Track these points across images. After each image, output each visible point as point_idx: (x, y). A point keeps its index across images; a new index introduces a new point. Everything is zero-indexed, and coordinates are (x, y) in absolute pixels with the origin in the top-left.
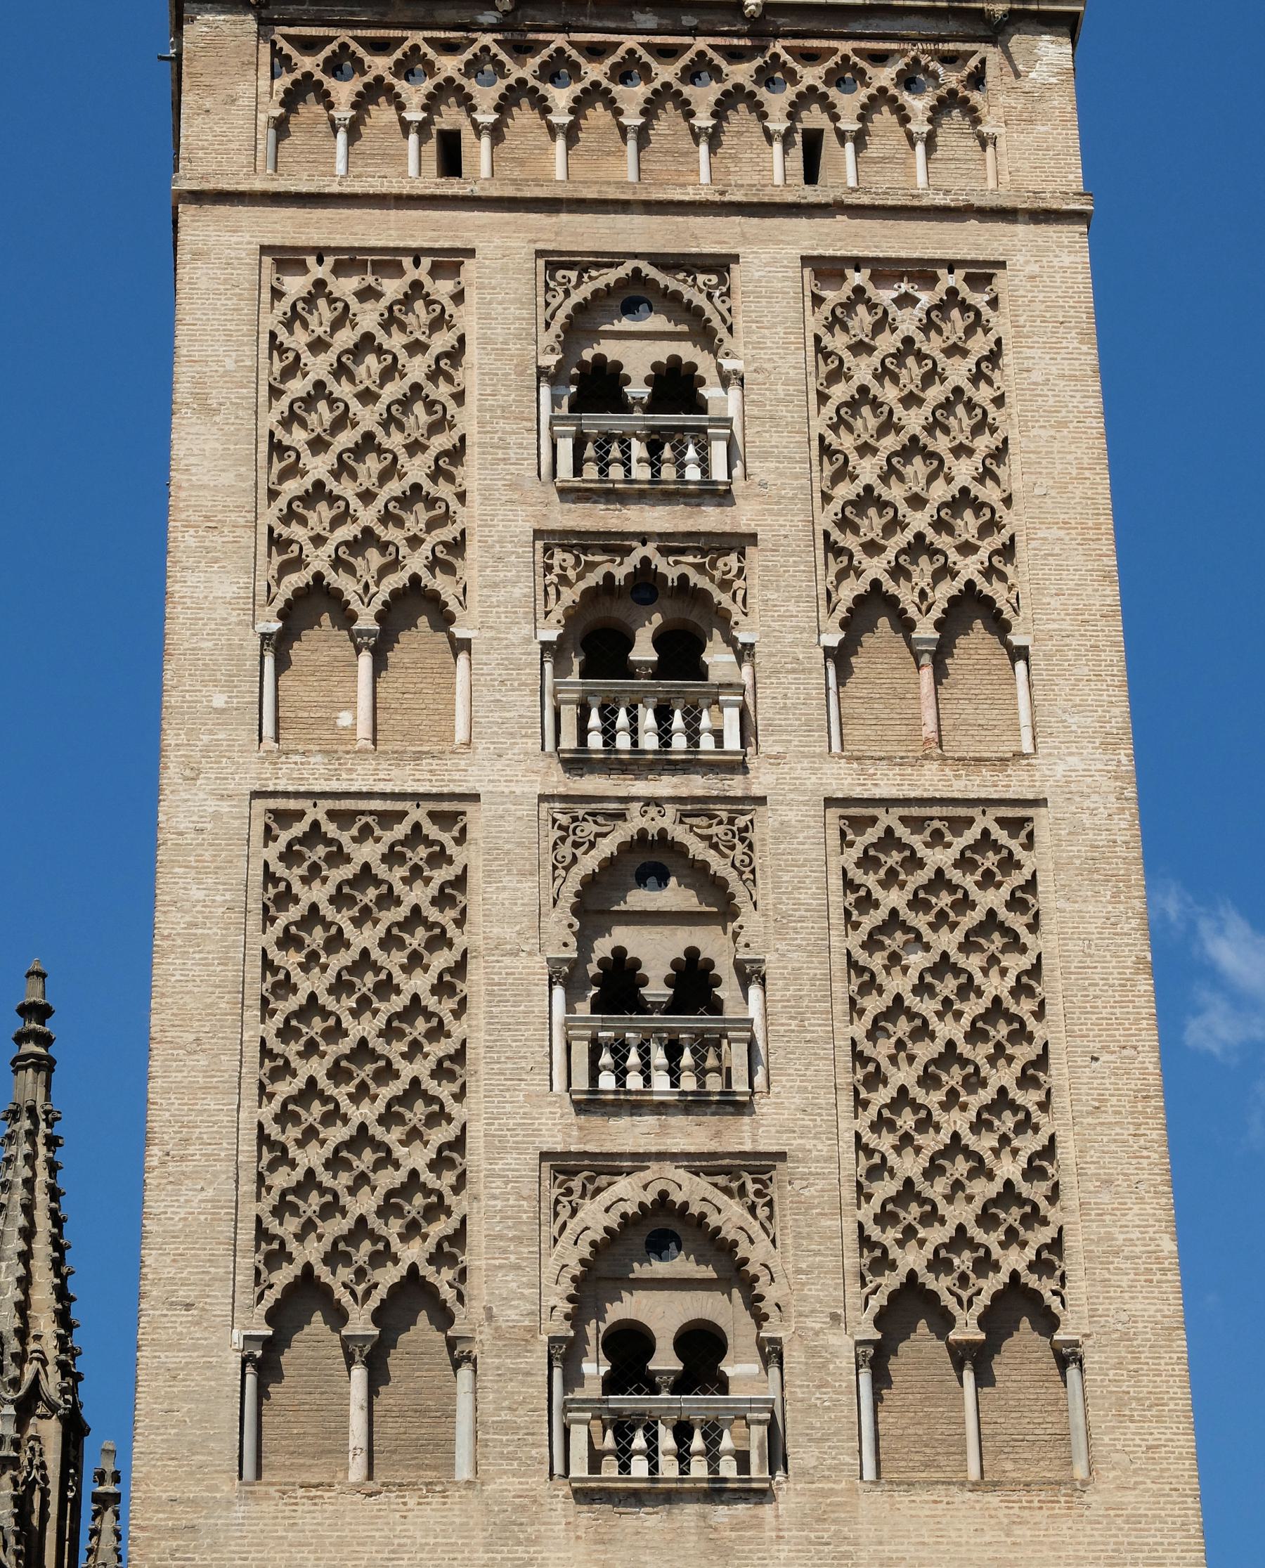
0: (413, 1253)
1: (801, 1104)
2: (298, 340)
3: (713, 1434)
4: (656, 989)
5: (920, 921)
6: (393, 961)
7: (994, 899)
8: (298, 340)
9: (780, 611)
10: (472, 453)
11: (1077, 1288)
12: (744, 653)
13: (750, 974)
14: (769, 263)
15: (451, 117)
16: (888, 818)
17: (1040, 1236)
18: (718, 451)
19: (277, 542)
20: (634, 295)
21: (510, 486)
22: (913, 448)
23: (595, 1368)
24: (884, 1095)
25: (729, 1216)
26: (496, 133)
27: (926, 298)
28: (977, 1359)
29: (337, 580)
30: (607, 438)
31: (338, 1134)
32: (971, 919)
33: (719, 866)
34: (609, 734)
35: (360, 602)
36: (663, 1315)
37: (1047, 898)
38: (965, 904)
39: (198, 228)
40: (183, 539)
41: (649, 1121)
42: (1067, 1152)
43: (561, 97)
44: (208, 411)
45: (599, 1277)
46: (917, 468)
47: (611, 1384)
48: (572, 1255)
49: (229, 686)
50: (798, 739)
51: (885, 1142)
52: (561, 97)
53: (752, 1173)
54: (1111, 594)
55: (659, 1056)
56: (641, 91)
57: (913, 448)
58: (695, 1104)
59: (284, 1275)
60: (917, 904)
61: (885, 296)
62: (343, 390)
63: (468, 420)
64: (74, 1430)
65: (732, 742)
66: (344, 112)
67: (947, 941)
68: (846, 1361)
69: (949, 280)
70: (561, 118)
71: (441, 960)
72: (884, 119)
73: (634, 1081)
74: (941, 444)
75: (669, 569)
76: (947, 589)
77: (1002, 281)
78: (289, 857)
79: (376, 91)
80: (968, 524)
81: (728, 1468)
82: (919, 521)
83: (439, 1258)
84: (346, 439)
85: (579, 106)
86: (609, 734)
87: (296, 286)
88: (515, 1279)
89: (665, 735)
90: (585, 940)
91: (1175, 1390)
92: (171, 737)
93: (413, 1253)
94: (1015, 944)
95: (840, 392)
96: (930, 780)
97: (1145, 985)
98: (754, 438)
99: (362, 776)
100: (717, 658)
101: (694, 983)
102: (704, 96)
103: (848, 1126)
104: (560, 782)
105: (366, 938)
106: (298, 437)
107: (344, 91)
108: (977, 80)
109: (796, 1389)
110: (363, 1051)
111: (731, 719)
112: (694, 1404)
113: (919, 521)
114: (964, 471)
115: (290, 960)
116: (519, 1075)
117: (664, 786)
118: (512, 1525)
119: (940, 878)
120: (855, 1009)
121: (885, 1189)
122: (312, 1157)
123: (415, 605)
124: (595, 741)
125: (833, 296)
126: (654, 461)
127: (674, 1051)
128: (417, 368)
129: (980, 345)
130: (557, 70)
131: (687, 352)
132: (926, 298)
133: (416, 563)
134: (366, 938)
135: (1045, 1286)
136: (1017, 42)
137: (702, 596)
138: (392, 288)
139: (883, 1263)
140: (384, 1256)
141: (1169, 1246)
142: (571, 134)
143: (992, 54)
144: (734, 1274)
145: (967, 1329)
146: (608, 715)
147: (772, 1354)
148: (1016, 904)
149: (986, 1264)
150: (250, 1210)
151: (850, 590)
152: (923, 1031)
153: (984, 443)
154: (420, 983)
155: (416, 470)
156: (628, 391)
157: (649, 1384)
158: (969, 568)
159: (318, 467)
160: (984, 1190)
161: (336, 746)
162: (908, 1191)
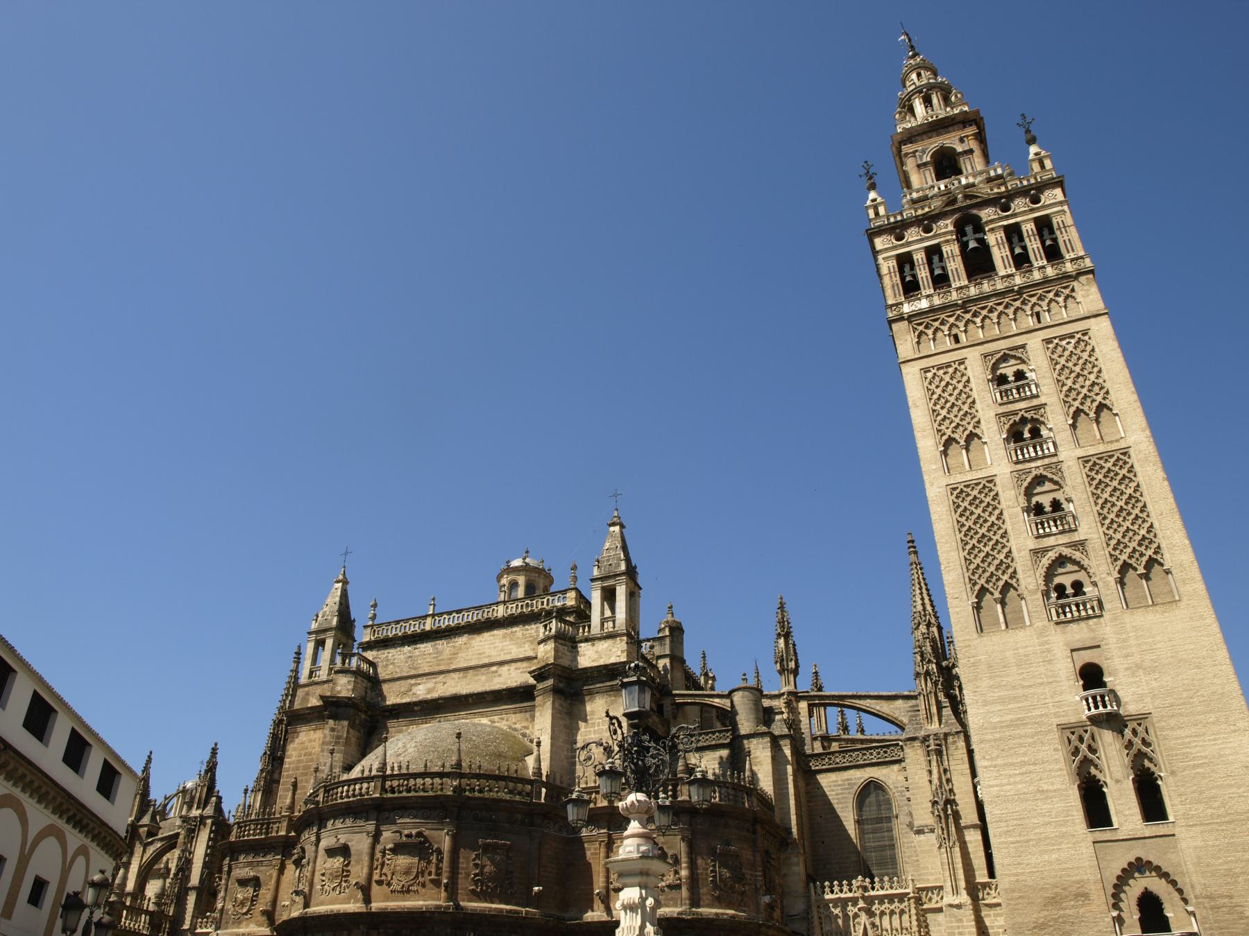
1: (1089, 528)
2: (933, 387)
3: (1084, 604)
4: (1048, 509)
7: (1124, 471)
9: (1056, 421)
11: (1167, 556)
12: (1050, 430)
13: (1069, 500)
14: (1034, 342)
16: (1094, 459)
17: (1154, 546)
18: (1033, 387)
20: (1005, 358)
22: (1078, 376)
23: (1054, 595)
24: (1107, 522)
25: (1077, 555)
26: (966, 331)
27: (1073, 341)
28: (1146, 576)
30: (1006, 391)
31: (982, 555)
32: (1119, 477)
33: (1055, 478)
34: (1023, 454)
35: (960, 438)
37: (1137, 468)
38: (1117, 474)
39: (906, 369)
40: (918, 434)
42: (1156, 525)
43: (978, 320)
45: (1049, 575)
46: (1081, 379)
47: (1058, 598)
48: (1041, 571)
50: (1067, 448)
51: (1111, 532)
52: (978, 320)
53: (1080, 545)
54: (1135, 397)
55: (1052, 523)
56: (996, 314)
57: (1078, 376)
58: (1062, 533)
59: (977, 588)
60: (1105, 477)
61: (1064, 343)
63: (975, 394)
64: (940, 628)
65: (1052, 450)
66: (931, 336)
67: (1115, 483)
68: (1113, 583)
70: (979, 324)
71: (997, 512)
72: (1053, 304)
73: (1047, 530)
74: (1085, 372)
75: (1028, 415)
76: (1095, 404)
77: (1090, 333)
78: (957, 497)
79: (937, 330)
81: (1090, 612)
82: (1084, 391)
83: (1011, 577)
84: (948, 405)
85: (983, 321)
86: (1023, 454)
87: (929, 375)
88: (1030, 579)
89: (1036, 452)
90: (1029, 501)
92: (925, 477)
94: (1131, 480)
95: (1058, 367)
96: (1102, 448)
97: (1166, 483)
98: (1040, 382)
99: (969, 476)
100: (1044, 432)
101: (1056, 505)
102: (1010, 311)
103: (1101, 530)
105: (979, 511)
106: (938, 407)
107: (930, 332)
108: (1073, 290)
109: (1102, 591)
110: (983, 536)
111: (1051, 445)
112: (1078, 599)
113: (1084, 391)
114: (1092, 377)
116: (1021, 535)
117: (1039, 463)
119: (1110, 471)
120: (1096, 504)
121: (1113, 542)
123: (971, 437)
124: (1020, 457)
125: (1051, 346)
126: (1019, 393)
127: (1055, 521)
129: (1089, 348)
130: (975, 315)
131: (1021, 367)
132: (1073, 341)
133: (970, 428)
135: (1158, 557)
137: (1037, 420)
138: (951, 370)
139: (1116, 559)
141: (1187, 542)
142: (982, 327)
143: (1075, 284)
144: (1082, 567)
145: (1141, 570)
146: (1022, 451)
147: (1095, 584)
148: (1129, 471)
150: (966, 575)
151: (1072, 410)
152: (1113, 505)
153: (1096, 370)
155: (966, 408)
156: (1007, 378)
157: (1067, 597)
158: (1099, 398)
159: (944, 412)
160: (1138, 538)
162: (1119, 542)
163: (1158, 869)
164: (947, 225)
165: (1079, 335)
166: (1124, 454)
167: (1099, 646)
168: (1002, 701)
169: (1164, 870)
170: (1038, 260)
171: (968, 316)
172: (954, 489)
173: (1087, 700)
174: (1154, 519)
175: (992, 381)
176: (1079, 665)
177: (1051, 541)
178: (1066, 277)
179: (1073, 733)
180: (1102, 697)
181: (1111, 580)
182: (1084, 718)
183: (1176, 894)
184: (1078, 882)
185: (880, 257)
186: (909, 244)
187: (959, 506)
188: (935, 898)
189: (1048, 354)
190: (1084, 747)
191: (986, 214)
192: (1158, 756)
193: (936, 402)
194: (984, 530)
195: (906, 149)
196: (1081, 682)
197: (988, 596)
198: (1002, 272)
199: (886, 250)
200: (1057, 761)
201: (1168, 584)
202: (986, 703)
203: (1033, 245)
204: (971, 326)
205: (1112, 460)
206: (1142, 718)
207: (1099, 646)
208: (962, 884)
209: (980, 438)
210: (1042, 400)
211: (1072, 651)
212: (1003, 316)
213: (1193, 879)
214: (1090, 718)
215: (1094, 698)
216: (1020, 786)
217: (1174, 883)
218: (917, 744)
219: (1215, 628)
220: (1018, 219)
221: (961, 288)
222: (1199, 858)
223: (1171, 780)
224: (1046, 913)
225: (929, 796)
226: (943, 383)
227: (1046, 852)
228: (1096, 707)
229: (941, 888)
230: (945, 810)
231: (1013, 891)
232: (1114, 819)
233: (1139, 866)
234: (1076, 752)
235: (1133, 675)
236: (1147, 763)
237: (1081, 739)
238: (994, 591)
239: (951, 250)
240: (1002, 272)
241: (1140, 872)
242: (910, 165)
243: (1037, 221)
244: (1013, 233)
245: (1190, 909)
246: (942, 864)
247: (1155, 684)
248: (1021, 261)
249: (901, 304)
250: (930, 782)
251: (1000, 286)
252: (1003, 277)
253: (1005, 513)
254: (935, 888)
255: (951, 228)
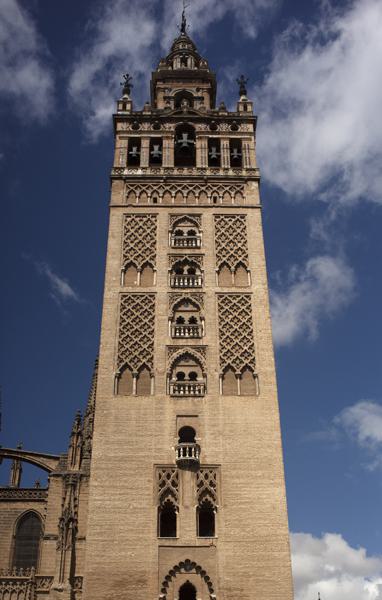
0: (144, 361)
1: (210, 337)
3: (194, 387)
5: (231, 311)
6: (142, 317)
8: (129, 227)
9: (209, 265)
10: (158, 243)
11: (257, 366)
13: (202, 319)
14: (207, 216)
15: (155, 195)
18: (198, 241)
19: (125, 256)
20: (185, 219)
21: (163, 248)
23: (174, 379)
25: (198, 355)
29: (134, 261)
30: (179, 240)
31: (132, 343)
36: (187, 371)
37: (253, 308)
38: (239, 308)
39: (113, 211)
41: (184, 340)
44: (114, 237)
48: (171, 361)
49: (116, 276)
50: (211, 283)
51: (224, 344)
52: (173, 193)
53: (203, 349)
54: (264, 263)
56: (187, 191)
61: (227, 220)
62: (136, 234)
63: (157, 238)
67: (236, 314)
68: (217, 377)
69: (237, 217)
70: (173, 195)
75: (190, 259)
80: (240, 252)
81: (197, 393)
83: (148, 361)
84: (137, 241)
88: (161, 364)
91: (274, 379)
92: (106, 284)
93: (144, 361)
95: (219, 234)
96: (233, 290)
99: (138, 290)
100: (198, 273)
101: (193, 320)
102: (197, 192)
104: (171, 290)
105: (138, 314)
106: (129, 241)
107: (138, 192)
108: (242, 189)
110: (137, 330)
115: (125, 317)
116: (163, 334)
118: (160, 401)
120: (220, 324)
122: (128, 346)
128: (149, 231)
134: (138, 314)
135: (251, 365)
136: (249, 183)
138: (145, 219)
139: (224, 362)
140: (139, 361)
146: (179, 281)
147: (205, 376)
148: (247, 308)
149: (242, 362)
151: (220, 263)
153: (243, 241)
154: (147, 320)
155: (148, 246)
156: (184, 232)
159: (132, 245)
161: (134, 286)
163: (199, 569)
164: (170, 127)
165: (237, 217)
166: (247, 297)
167: (196, 416)
168: (119, 443)
169: (203, 569)
170: (225, 163)
171: (168, 188)
172: (125, 296)
173: (179, 450)
174: (255, 341)
175: (172, 232)
176: (182, 426)
177: (181, 342)
178: (241, 179)
179: (164, 472)
180: (190, 449)
181: (217, 375)
182: (174, 462)
183: (206, 586)
184: (141, 572)
185: (118, 136)
186: (141, 132)
187: (124, 308)
188: (47, 583)
189: (215, 223)
190: (169, 482)
191: (199, 127)
192: (218, 495)
193: (129, 237)
194: (138, 327)
195: (160, 85)
196: (179, 438)
197: (128, 370)
198: (199, 165)
199: (124, 132)
200: (148, 489)
201: (254, 384)
202: (107, 442)
203: (225, 155)
204: (167, 195)
205: (238, 299)
206: (214, 467)
207: (196, 416)
208: (68, 576)
209: (152, 267)
210: (202, 251)
211: (178, 416)
212: (191, 194)
213: (222, 576)
214: (178, 463)
215: (184, 449)
216: (117, 503)
217: (207, 579)
218: (59, 479)
219: (277, 416)
220: (220, 136)
221: (168, 168)
222: (228, 563)
223: (223, 524)
224: (113, 591)
225: (60, 515)
226: (137, 227)
227: (124, 549)
228: (184, 455)
229: (52, 578)
230: (67, 525)
231: (94, 574)
232: (178, 533)
233: (188, 565)
234: (163, 484)
235: (215, 438)
236: (208, 497)
237: (168, 476)
238: (135, 368)
239: (169, 145)
240: (198, 166)
241: (186, 569)
242: (161, 95)
243: (232, 141)
244: (214, 144)
245: (213, 596)
246: (57, 561)
247: (228, 446)
248: (214, 162)
249: (123, 168)
250: (63, 505)
251: (195, 173)
252: (198, 169)
253: (156, 319)
254: (49, 577)
255: (172, 129)
